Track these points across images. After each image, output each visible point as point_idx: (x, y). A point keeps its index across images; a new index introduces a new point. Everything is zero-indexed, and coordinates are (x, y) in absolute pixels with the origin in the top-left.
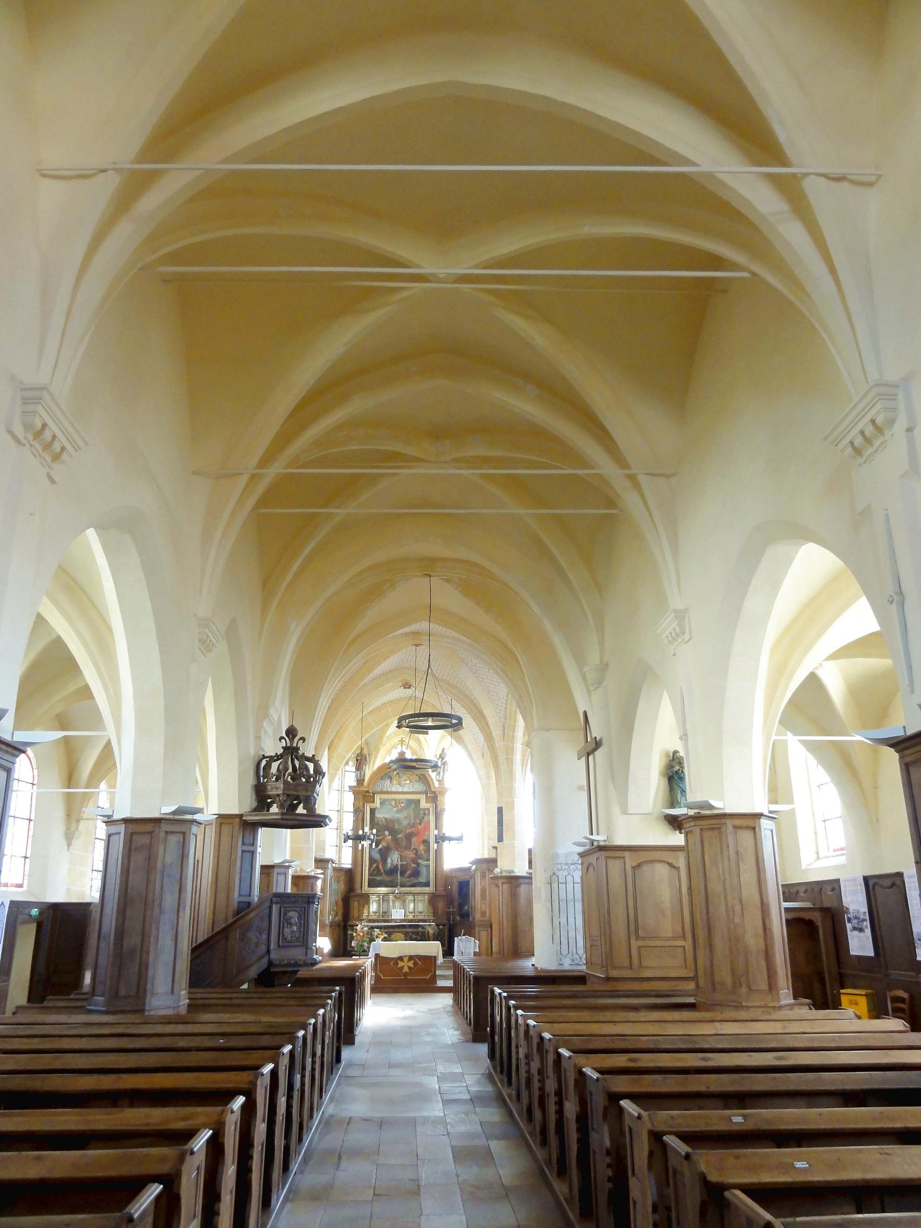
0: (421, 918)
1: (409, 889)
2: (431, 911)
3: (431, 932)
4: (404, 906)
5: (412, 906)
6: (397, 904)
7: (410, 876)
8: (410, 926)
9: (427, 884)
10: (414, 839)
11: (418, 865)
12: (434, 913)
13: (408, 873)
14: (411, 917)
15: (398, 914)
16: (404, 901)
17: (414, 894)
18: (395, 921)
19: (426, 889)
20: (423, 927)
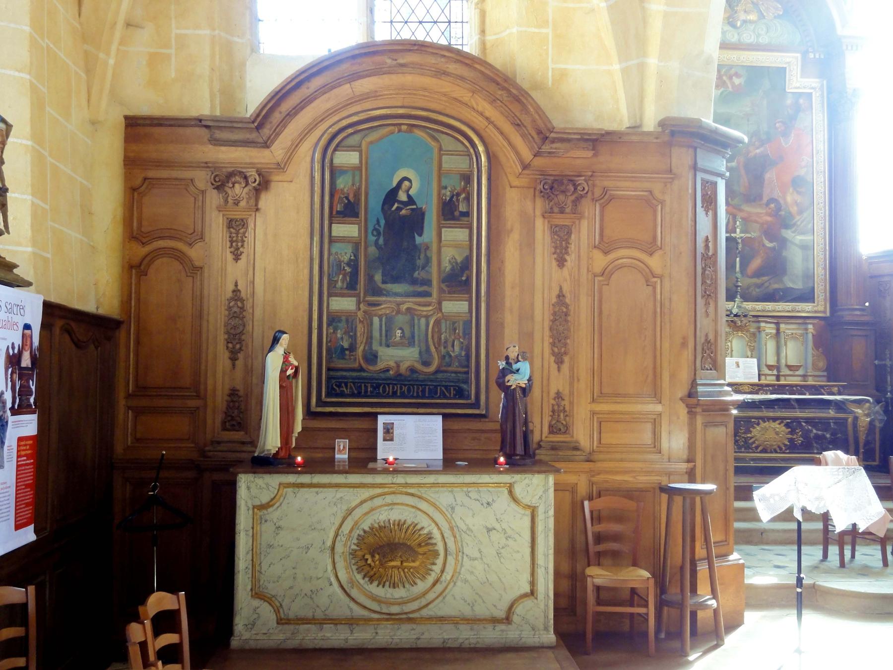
0: (795, 381)
1: (760, 306)
2: (822, 364)
3: (865, 421)
4: (755, 351)
5: (771, 346)
6: (737, 343)
7: (758, 274)
9: (807, 296)
10: (770, 175)
11: (783, 243)
13: (756, 263)
14: (771, 380)
16: (755, 336)
17: (778, 320)
19: (805, 309)
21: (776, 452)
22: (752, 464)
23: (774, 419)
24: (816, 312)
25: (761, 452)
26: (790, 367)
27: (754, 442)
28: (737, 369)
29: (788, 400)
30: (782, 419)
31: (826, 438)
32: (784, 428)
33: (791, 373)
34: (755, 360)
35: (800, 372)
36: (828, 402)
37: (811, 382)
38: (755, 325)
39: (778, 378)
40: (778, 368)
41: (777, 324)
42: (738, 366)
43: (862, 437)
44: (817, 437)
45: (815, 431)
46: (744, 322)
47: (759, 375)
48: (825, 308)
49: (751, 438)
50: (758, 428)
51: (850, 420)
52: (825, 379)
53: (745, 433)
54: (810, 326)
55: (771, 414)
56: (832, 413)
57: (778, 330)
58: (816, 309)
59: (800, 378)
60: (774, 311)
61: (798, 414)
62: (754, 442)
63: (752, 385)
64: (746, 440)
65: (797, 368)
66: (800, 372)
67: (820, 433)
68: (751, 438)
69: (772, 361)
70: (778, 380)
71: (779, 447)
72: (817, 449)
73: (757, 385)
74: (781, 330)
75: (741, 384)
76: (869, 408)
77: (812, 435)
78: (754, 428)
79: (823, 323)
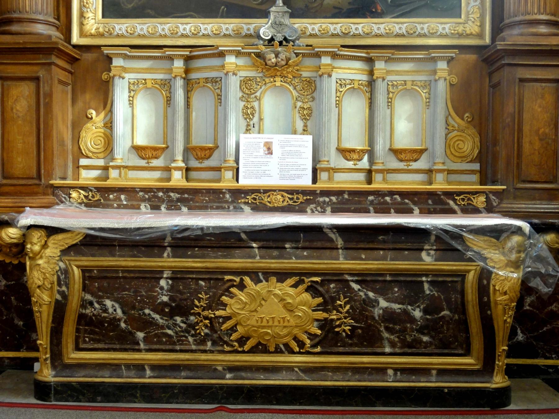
2: (469, 145)
3: (507, 277)
4: (308, 118)
5: (354, 110)
6: (273, 103)
8: (359, 238)
12: (480, 158)
14: (349, 180)
15: (273, 155)
16: (311, 87)
17: (369, 53)
18: (256, 198)
20: (449, 244)
21: (292, 352)
22: (229, 380)
23: (282, 276)
24: (461, 36)
25: (252, 351)
26: (396, 152)
27: (233, 329)
28: (268, 158)
29: (317, 229)
30: (300, 276)
31: (412, 320)
32: (307, 296)
33: (401, 165)
34: (308, 139)
35: (422, 164)
36: (421, 234)
37: (440, 184)
38: (310, 62)
39: (369, 172)
40: (371, 153)
41: (370, 61)
42: (269, 151)
43: (503, 318)
44: (389, 317)
45: (383, 303)
46: (282, 56)
47: (315, 171)
48: (482, 26)
49: (228, 318)
50: (242, 296)
51: (471, 277)
52: (475, 178)
53: (209, 307)
54: (442, 65)
55: (274, 264)
56: (428, 259)
57: (371, 73)
58: (460, 29)
59: (420, 177)
60: (368, 35)
61: (343, 262)
62: (233, 329)
63: (291, 191)
64: (213, 324)
65: (416, 154)
66: (422, 164)
67: (396, 307)
68: (228, 318)
69: (354, 139)
70: (369, 181)
71: (295, 339)
72: (393, 344)
73: (304, 192)
74: (377, 74)
75: (267, 191)
76: (521, 248)
77: (377, 312)
78: (232, 296)
79: (472, 57)
